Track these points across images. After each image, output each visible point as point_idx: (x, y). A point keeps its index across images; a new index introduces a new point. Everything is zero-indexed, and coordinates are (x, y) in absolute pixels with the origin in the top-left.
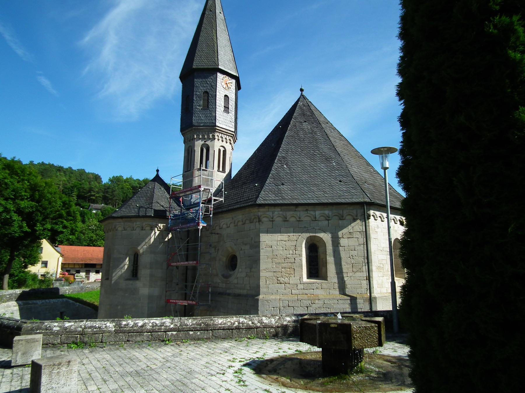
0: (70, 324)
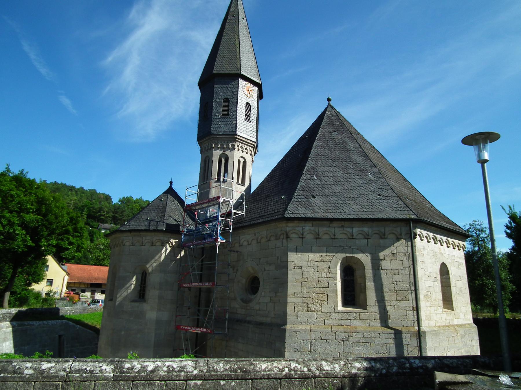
0: (50, 365)
